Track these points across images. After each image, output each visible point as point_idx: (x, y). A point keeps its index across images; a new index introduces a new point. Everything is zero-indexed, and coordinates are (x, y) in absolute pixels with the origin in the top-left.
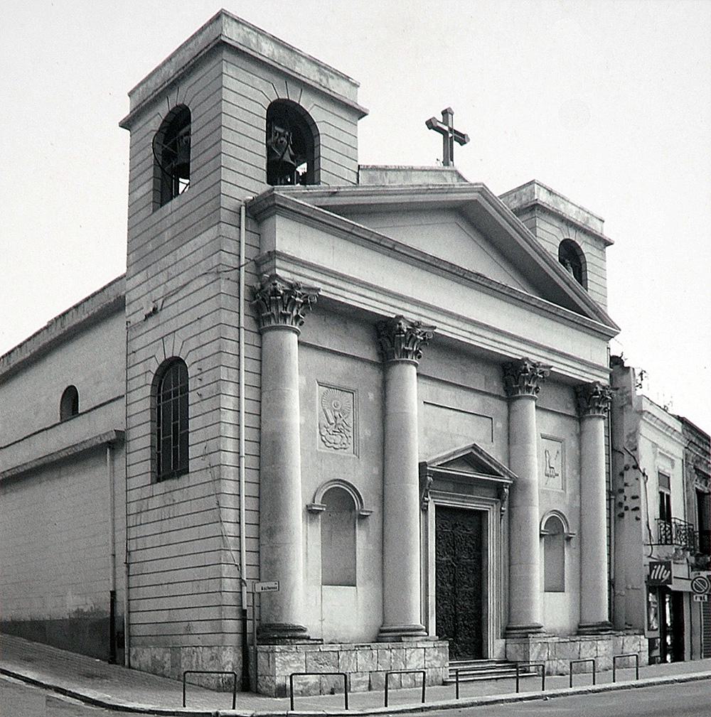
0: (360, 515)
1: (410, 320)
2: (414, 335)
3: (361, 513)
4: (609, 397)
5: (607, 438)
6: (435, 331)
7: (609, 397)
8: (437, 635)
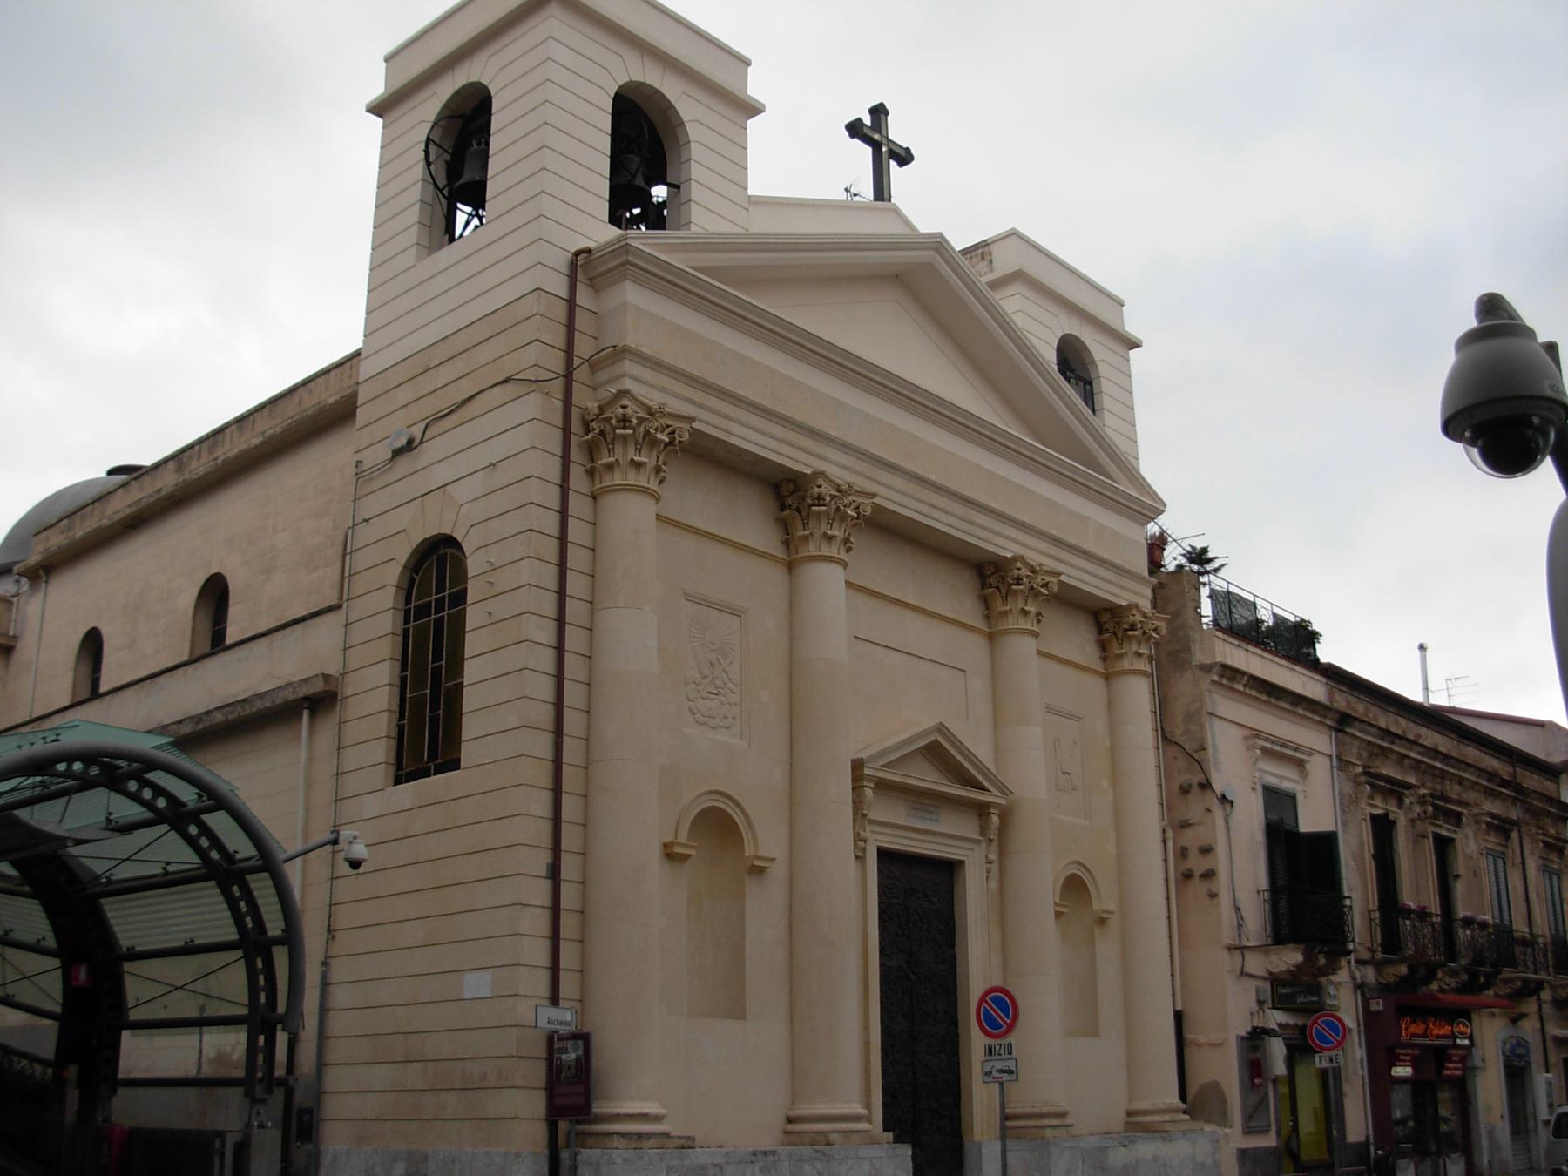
0: (753, 865)
1: (835, 479)
2: (842, 507)
3: (756, 863)
4: (1043, 590)
5: (1153, 714)
6: (875, 500)
7: (1043, 590)
8: (886, 1129)
